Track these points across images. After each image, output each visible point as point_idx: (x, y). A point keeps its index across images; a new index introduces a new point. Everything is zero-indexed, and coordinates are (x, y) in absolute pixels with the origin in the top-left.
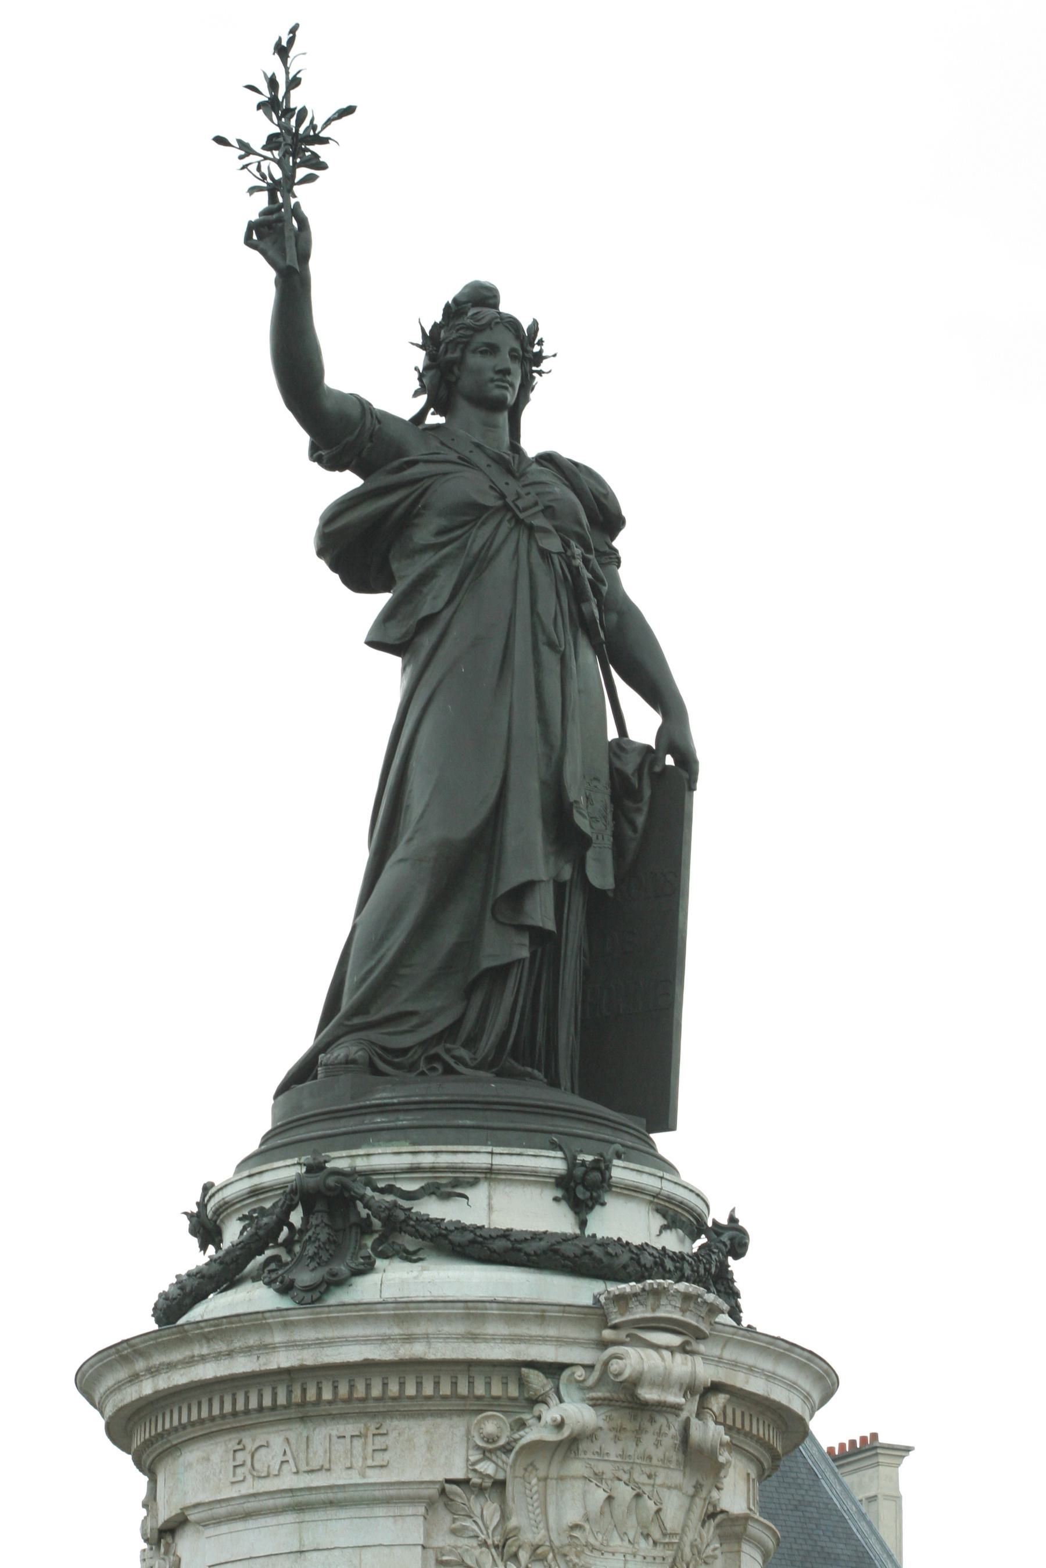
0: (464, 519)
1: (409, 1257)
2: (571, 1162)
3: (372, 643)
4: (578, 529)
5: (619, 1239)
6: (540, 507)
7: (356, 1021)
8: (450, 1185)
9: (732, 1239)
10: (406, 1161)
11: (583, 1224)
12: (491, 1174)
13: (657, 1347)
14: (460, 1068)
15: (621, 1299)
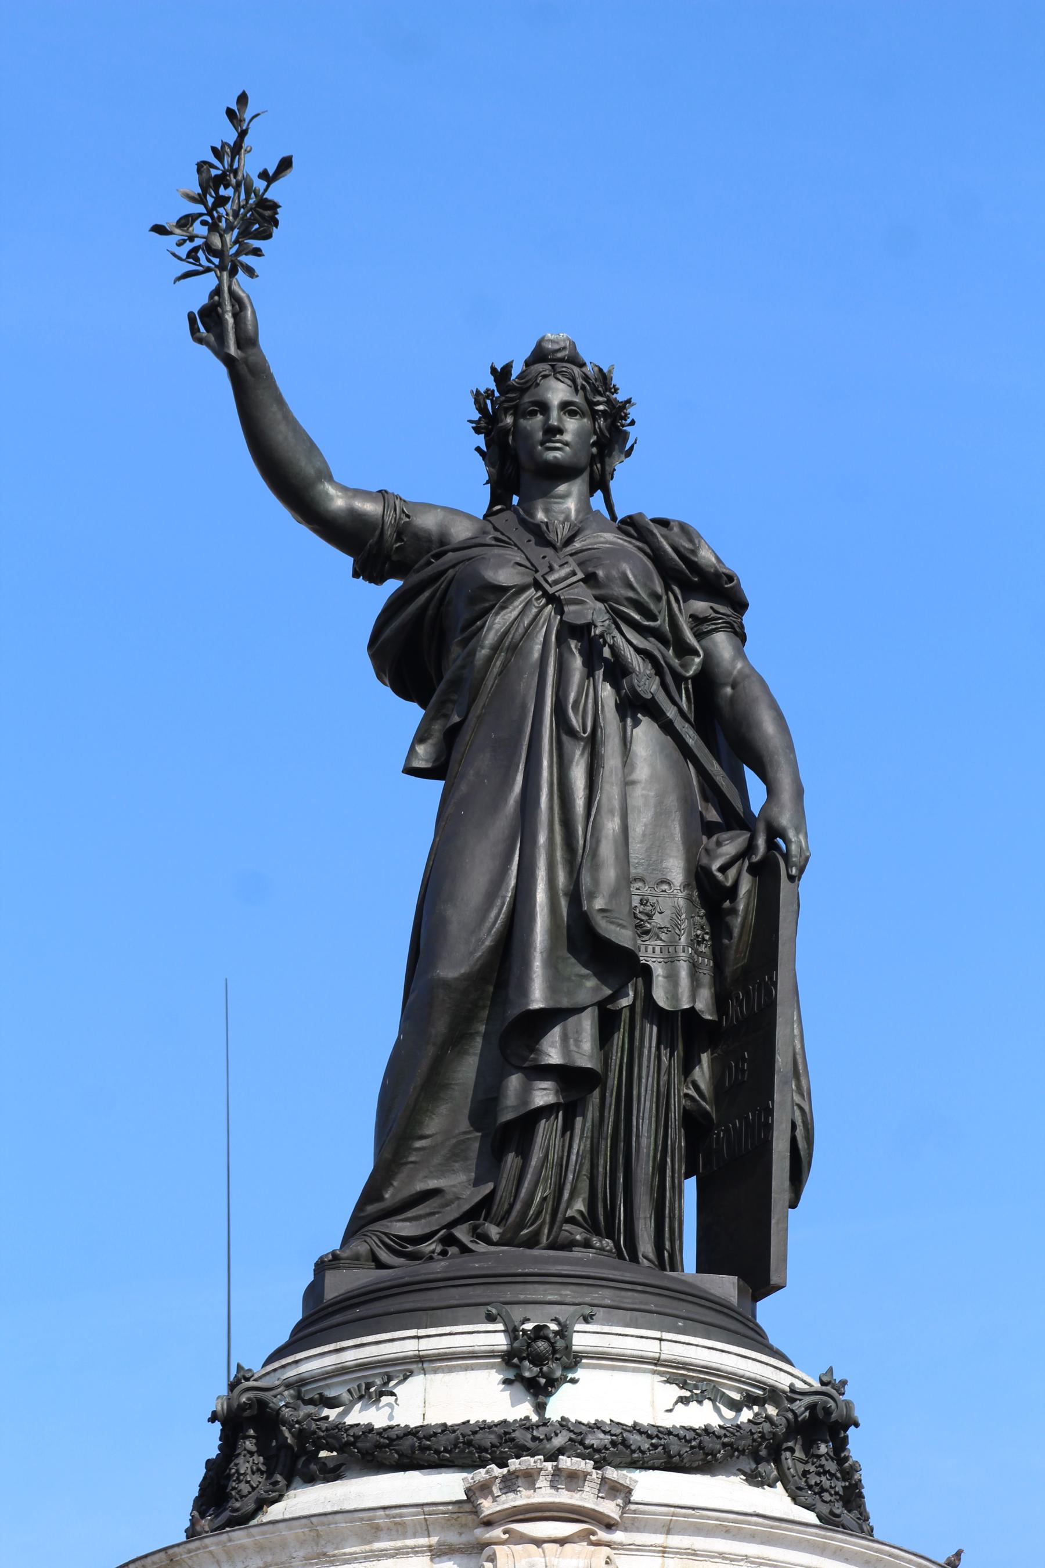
0: (530, 607)
1: (332, 1473)
2: (512, 1332)
3: (410, 771)
4: (631, 594)
5: (635, 1424)
6: (580, 575)
7: (371, 1209)
8: (377, 1381)
9: (812, 1407)
10: (329, 1362)
11: (540, 1408)
12: (422, 1362)
13: (538, 1542)
14: (481, 1247)
15: (484, 1488)
